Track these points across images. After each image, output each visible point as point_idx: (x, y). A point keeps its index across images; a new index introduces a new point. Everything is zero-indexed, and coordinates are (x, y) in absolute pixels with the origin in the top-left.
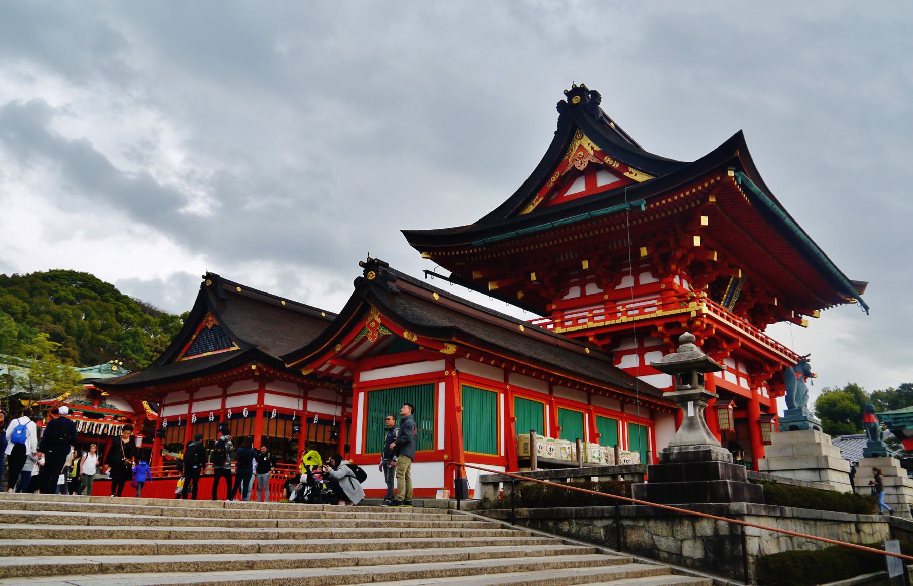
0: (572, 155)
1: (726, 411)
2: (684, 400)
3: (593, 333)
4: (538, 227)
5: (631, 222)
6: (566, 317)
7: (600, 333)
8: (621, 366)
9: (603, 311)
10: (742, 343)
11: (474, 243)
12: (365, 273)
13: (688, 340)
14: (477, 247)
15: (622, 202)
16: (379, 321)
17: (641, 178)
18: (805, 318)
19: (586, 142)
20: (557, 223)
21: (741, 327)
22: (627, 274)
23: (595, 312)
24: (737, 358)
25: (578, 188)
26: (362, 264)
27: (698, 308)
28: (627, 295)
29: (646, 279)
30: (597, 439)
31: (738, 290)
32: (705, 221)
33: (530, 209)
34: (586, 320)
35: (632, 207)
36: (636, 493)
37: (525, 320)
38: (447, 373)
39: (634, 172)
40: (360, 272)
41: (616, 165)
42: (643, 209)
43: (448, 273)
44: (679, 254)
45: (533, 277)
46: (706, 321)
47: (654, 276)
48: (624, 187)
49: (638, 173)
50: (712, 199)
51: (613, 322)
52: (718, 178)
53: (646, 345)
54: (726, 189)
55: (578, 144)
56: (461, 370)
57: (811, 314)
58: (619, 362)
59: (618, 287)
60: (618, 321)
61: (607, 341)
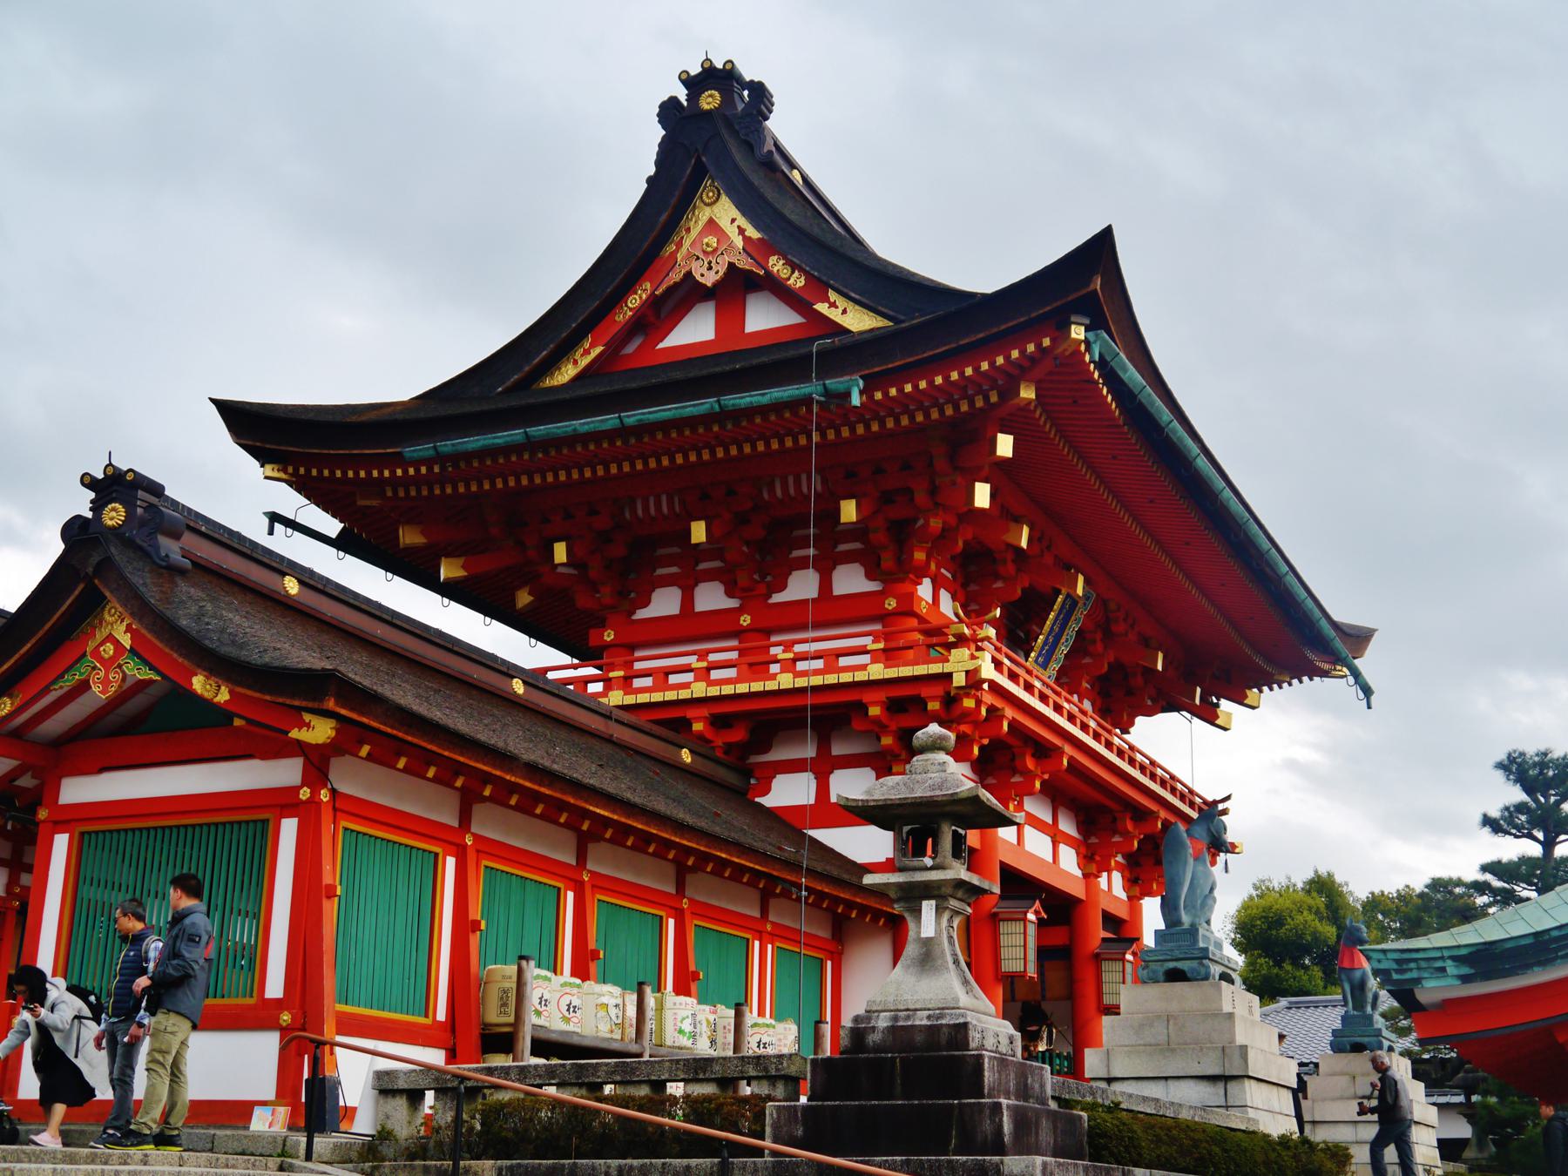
0: (687, 244)
1: (1019, 927)
2: (914, 894)
3: (705, 712)
4: (582, 425)
5: (823, 435)
6: (638, 666)
7: (723, 712)
8: (768, 801)
9: (734, 655)
10: (1071, 759)
11: (410, 451)
12: (97, 506)
13: (935, 746)
14: (417, 464)
15: (805, 378)
16: (126, 641)
17: (857, 320)
18: (1226, 705)
19: (726, 213)
20: (633, 417)
21: (1071, 718)
22: (802, 564)
23: (713, 657)
24: (1057, 796)
25: (696, 329)
26: (88, 482)
27: (971, 665)
28: (796, 618)
29: (851, 581)
30: (694, 987)
31: (1073, 628)
32: (1005, 446)
33: (566, 373)
34: (689, 677)
35: (827, 392)
36: (775, 1127)
37: (528, 666)
38: (305, 794)
39: (841, 302)
40: (81, 503)
41: (797, 281)
42: (856, 400)
43: (332, 526)
44: (936, 523)
45: (560, 552)
46: (988, 699)
47: (870, 576)
48: (812, 340)
49: (850, 306)
50: (1028, 393)
51: (757, 687)
52: (1046, 342)
53: (838, 750)
54: (1062, 373)
55: (704, 214)
56: (343, 788)
57: (1240, 699)
58: (766, 791)
59: (777, 598)
60: (771, 686)
61: (738, 735)
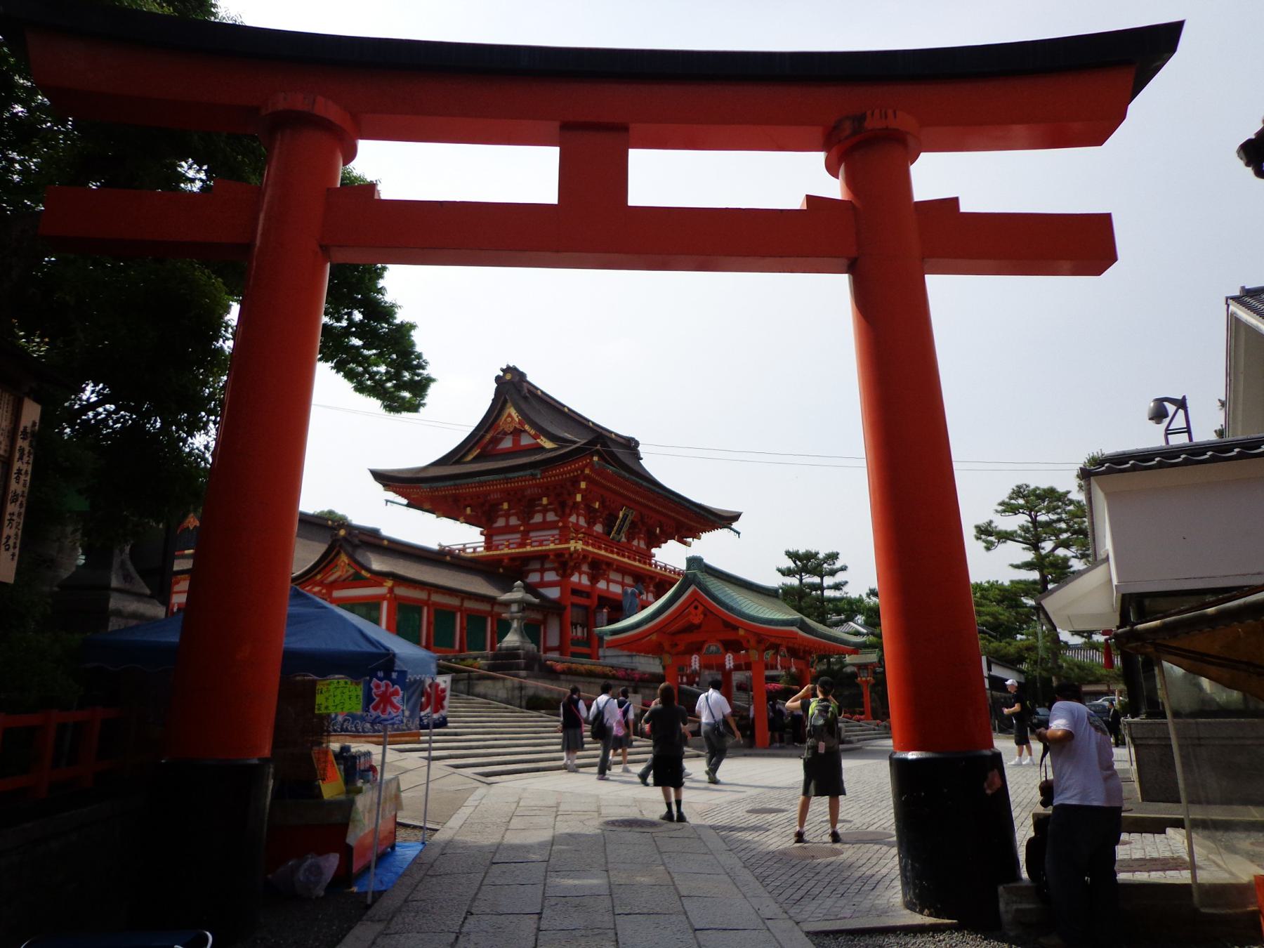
7: (513, 558)
17: (548, 445)
18: (690, 540)
22: (539, 511)
25: (507, 444)
31: (627, 522)
43: (405, 501)
